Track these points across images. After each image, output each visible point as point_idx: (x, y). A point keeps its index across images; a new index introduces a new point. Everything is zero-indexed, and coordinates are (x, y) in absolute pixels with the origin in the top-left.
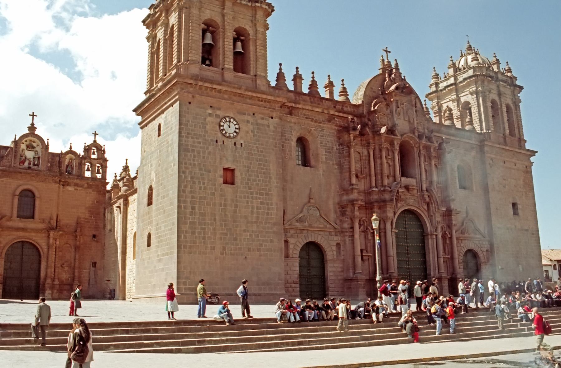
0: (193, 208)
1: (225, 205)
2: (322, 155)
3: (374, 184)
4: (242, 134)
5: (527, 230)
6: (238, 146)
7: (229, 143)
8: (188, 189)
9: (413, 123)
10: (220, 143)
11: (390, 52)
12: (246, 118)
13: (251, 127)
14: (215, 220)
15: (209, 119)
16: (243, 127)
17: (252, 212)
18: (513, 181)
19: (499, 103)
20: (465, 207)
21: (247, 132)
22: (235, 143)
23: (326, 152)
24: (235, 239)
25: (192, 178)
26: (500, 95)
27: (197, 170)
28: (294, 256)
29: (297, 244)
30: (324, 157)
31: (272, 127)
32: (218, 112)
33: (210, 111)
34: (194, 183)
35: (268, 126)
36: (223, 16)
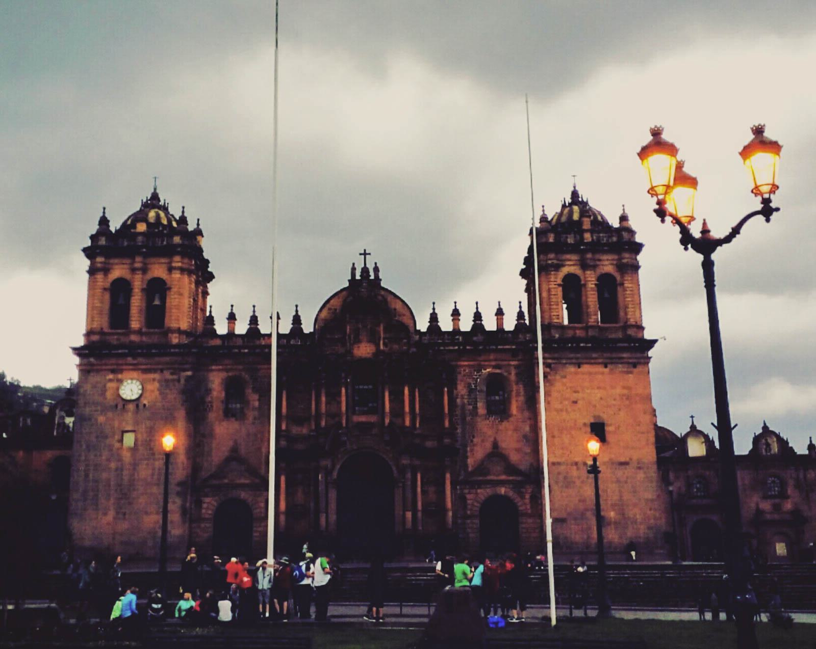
0: (87, 476)
1: (122, 470)
2: (254, 400)
3: (313, 427)
4: (147, 394)
5: (625, 464)
6: (141, 406)
7: (131, 407)
8: (83, 458)
9: (378, 345)
10: (120, 407)
11: (369, 254)
12: (152, 376)
13: (157, 385)
14: (109, 486)
15: (109, 385)
16: (149, 387)
17: (153, 475)
18: (596, 391)
19: (582, 278)
20: (492, 439)
21: (152, 391)
22: (137, 406)
23: (260, 396)
24: (130, 504)
25: (88, 446)
26: (584, 266)
27: (94, 439)
28: (207, 516)
29: (209, 505)
30: (257, 404)
31: (182, 381)
32: (120, 376)
33: (111, 376)
34: (89, 451)
35: (179, 381)
36: (133, 270)
